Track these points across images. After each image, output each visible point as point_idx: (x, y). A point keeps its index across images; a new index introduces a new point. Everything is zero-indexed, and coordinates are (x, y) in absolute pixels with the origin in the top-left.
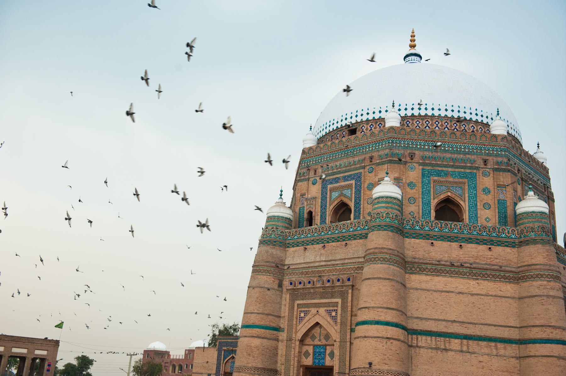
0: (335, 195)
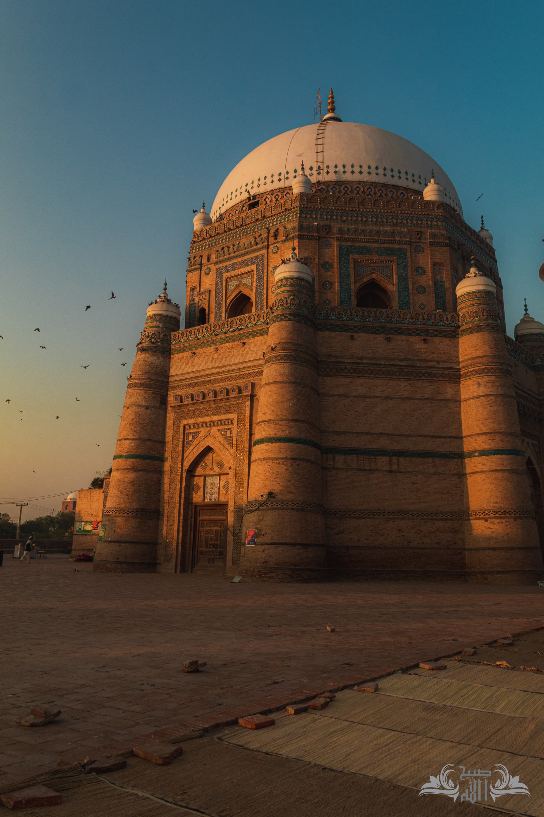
0: (232, 285)
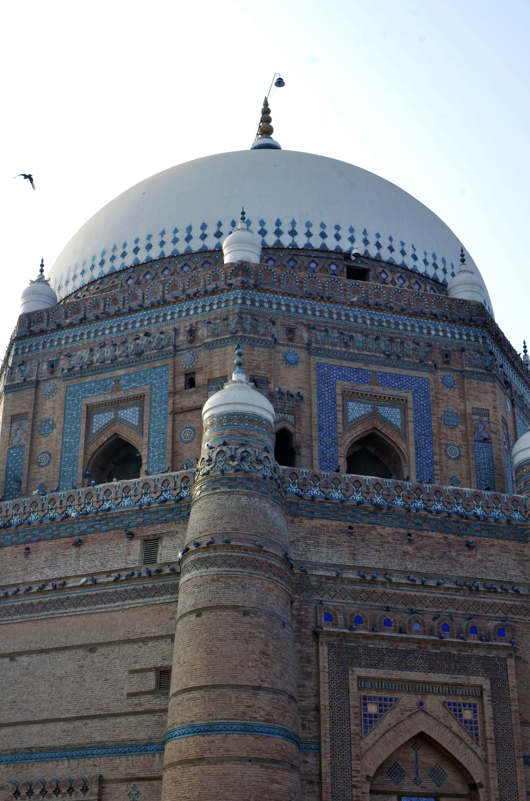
0: (357, 410)
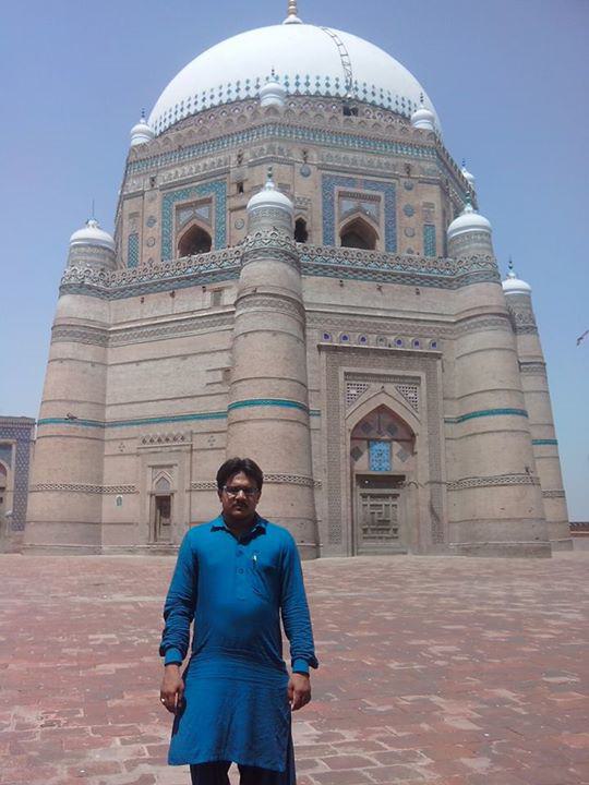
0: (349, 205)
